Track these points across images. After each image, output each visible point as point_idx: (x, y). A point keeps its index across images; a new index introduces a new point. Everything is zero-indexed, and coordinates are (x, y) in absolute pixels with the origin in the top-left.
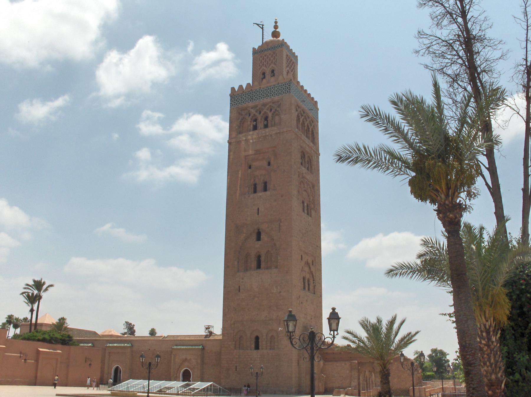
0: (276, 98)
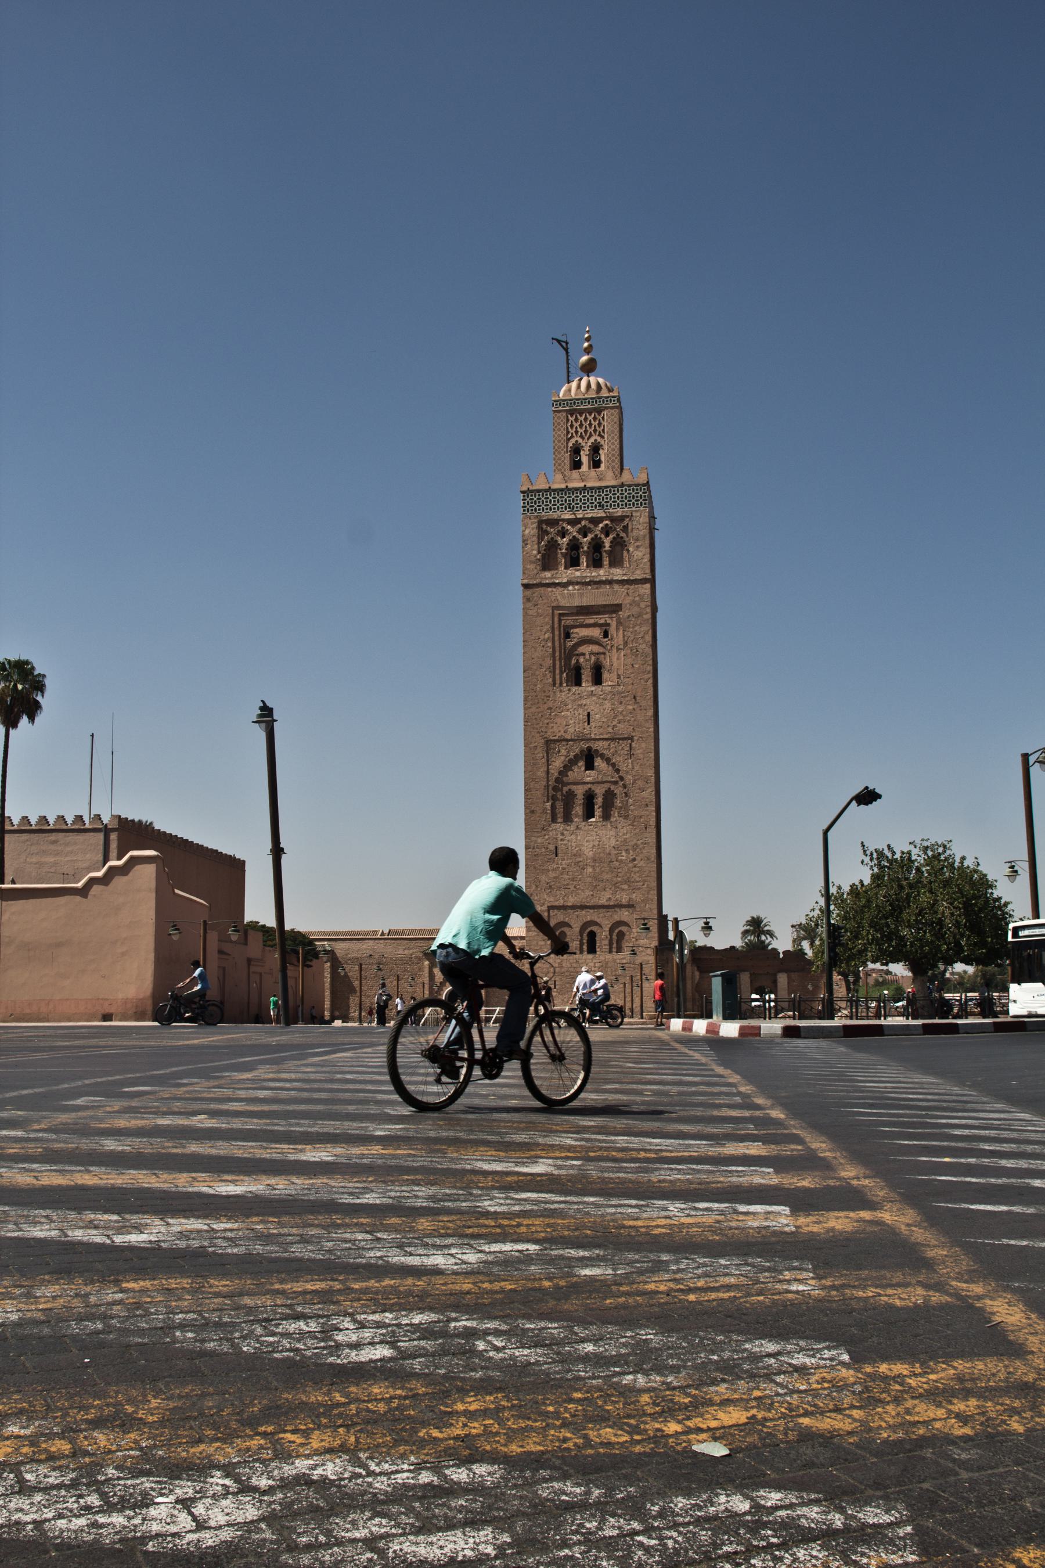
0: (619, 512)
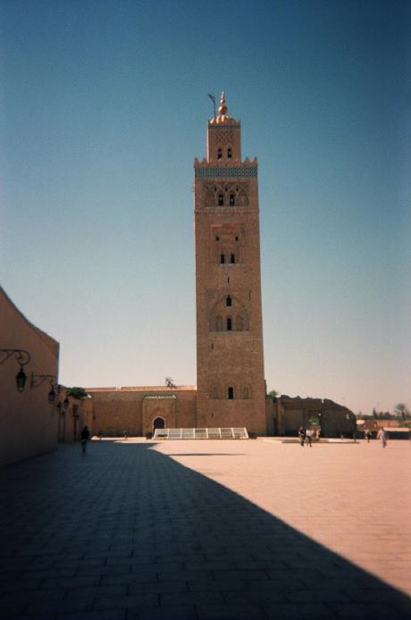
0: (243, 179)
